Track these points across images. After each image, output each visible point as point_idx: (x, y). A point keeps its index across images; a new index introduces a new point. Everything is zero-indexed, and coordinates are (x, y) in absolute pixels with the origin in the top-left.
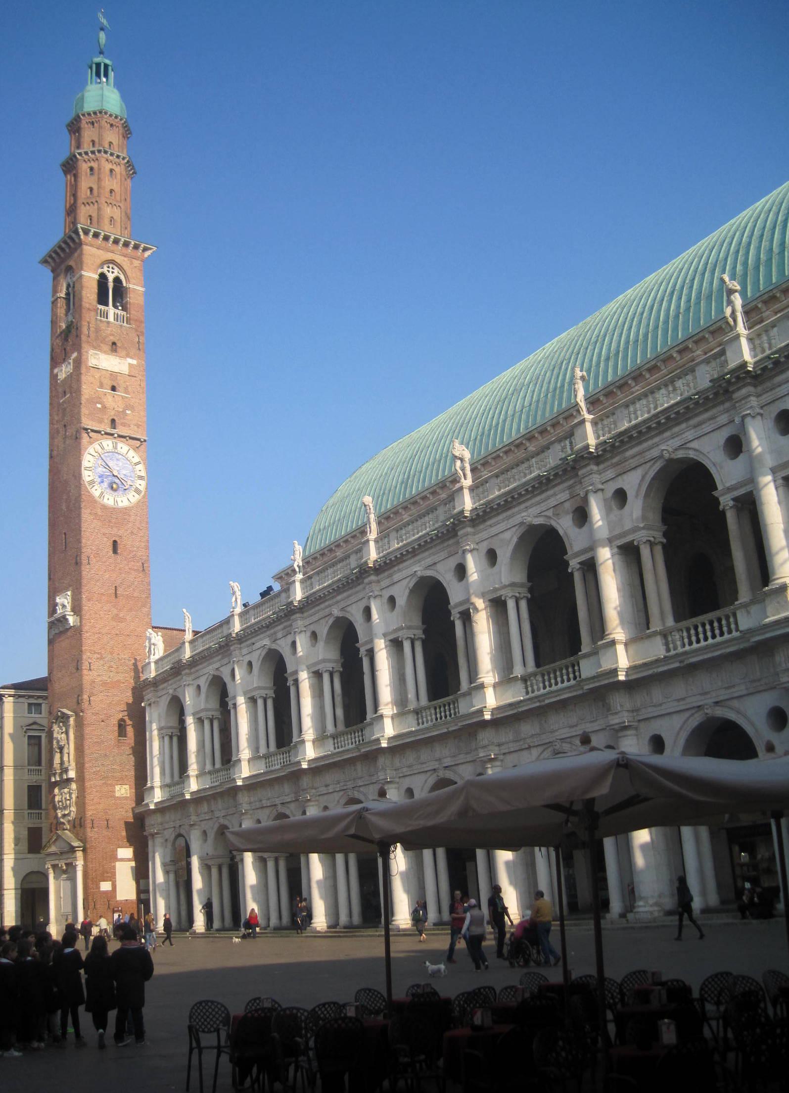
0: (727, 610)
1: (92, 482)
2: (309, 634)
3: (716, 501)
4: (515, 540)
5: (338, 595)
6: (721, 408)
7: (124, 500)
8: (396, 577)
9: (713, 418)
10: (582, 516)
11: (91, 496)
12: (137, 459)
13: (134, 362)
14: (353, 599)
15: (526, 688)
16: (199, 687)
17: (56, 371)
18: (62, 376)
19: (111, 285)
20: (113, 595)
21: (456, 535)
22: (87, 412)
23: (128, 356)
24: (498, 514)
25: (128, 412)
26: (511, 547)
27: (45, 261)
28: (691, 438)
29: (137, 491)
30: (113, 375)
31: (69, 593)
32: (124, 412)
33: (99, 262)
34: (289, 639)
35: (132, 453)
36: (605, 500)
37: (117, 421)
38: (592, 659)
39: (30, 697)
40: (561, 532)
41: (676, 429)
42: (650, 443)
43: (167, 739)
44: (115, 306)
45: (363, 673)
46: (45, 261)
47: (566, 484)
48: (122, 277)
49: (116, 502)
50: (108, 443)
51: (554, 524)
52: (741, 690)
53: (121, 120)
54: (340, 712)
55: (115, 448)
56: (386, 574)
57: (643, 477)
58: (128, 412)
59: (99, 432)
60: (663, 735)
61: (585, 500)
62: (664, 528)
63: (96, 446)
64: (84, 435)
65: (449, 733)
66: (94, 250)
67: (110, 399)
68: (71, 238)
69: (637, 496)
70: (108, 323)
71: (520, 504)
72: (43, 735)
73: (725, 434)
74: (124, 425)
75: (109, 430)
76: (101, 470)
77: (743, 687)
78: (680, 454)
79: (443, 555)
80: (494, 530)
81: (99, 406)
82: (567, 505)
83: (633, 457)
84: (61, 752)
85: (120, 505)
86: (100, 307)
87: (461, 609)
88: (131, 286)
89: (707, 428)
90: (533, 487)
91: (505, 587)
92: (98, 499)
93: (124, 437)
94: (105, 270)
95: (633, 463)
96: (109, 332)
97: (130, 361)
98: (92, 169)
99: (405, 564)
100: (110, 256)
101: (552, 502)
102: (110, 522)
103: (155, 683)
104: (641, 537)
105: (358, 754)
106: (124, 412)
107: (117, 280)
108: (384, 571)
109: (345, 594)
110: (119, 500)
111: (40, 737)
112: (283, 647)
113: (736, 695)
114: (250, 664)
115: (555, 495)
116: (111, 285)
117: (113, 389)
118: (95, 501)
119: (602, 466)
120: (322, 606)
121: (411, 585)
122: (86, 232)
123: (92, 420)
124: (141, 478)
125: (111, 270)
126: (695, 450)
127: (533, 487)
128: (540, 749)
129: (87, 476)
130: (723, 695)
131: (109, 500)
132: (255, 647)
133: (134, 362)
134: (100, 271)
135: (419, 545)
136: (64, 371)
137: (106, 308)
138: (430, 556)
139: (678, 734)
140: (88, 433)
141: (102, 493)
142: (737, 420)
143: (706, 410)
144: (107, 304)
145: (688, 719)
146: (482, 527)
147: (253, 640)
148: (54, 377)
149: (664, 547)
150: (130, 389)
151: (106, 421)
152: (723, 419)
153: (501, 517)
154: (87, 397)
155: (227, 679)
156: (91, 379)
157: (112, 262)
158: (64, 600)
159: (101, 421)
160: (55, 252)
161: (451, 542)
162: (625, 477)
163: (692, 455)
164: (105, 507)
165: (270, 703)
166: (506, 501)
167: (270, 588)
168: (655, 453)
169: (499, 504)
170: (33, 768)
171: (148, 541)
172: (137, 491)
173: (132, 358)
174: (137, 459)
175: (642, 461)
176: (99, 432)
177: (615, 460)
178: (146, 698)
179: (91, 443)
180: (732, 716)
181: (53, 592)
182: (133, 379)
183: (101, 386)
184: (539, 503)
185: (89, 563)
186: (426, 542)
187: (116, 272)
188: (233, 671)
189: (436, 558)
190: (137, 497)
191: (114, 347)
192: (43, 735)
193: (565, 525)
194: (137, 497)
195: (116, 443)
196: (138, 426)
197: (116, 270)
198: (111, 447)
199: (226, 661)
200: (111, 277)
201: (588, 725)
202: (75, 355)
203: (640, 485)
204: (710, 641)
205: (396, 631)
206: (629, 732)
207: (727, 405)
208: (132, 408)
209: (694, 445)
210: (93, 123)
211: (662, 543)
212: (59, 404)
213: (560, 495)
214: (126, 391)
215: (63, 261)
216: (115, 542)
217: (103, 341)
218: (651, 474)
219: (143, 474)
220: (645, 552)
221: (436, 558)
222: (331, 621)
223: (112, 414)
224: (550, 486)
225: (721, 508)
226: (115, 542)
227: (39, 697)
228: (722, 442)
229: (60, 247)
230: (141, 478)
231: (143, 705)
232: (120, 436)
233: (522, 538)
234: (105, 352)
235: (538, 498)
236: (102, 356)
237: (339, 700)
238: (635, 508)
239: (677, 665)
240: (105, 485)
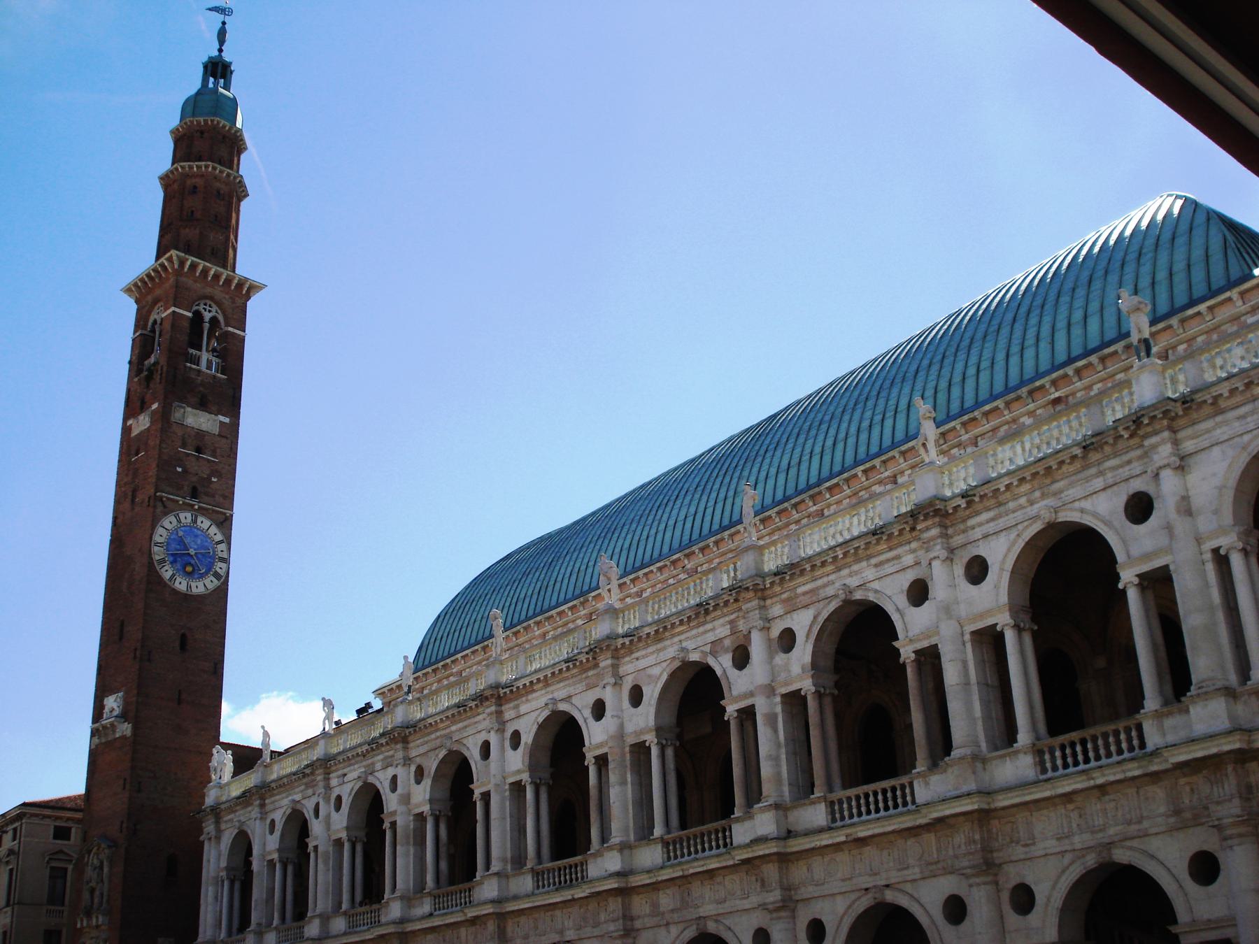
0: (904, 780)
1: (162, 561)
2: (413, 768)
3: (897, 653)
4: (665, 677)
5: (453, 723)
6: (907, 548)
7: (198, 587)
8: (524, 708)
9: (898, 557)
10: (742, 658)
12: (219, 537)
13: (227, 420)
14: (471, 731)
15: (668, 852)
16: (273, 821)
17: (129, 423)
18: (135, 433)
19: (206, 326)
21: (596, 666)
24: (648, 646)
26: (660, 685)
27: (128, 290)
28: (871, 577)
29: (217, 576)
30: (200, 434)
31: (120, 694)
34: (390, 772)
35: (214, 530)
36: (769, 640)
38: (747, 824)
39: (57, 818)
40: (719, 672)
41: (855, 567)
42: (825, 580)
43: (226, 883)
45: (476, 821)
46: (128, 290)
47: (727, 619)
48: (221, 318)
49: (189, 587)
50: (186, 517)
51: (711, 661)
52: (915, 872)
54: (444, 865)
55: (195, 522)
56: (512, 705)
57: (815, 617)
60: (824, 920)
61: (748, 637)
62: (836, 677)
64: (159, 504)
65: (573, 900)
68: (162, 265)
69: (808, 636)
70: (199, 371)
71: (673, 636)
72: (70, 867)
73: (910, 576)
74: (207, 494)
77: (917, 870)
78: (858, 596)
79: (580, 687)
80: (642, 663)
81: (179, 470)
82: (727, 642)
83: (805, 594)
84: (92, 891)
85: (195, 591)
86: (191, 351)
87: (599, 752)
88: (230, 329)
89: (889, 569)
90: (689, 617)
91: (651, 730)
93: (207, 509)
94: (201, 308)
95: (806, 599)
97: (222, 418)
98: (195, 187)
99: (534, 695)
100: (208, 290)
101: (710, 637)
103: (216, 811)
104: (806, 685)
105: (463, 919)
107: (214, 321)
108: (510, 700)
109: (460, 725)
110: (193, 585)
111: (66, 869)
112: (382, 780)
113: (910, 878)
114: (339, 799)
115: (713, 629)
116: (206, 326)
117: (199, 450)
119: (769, 602)
120: (433, 736)
121: (541, 720)
122: (182, 263)
126: (876, 591)
127: (689, 617)
128: (681, 927)
129: (158, 553)
130: (894, 877)
131: (181, 585)
132: (346, 779)
133: (227, 420)
134: (195, 308)
135: (553, 673)
136: (142, 423)
138: (564, 687)
139: (842, 918)
141: (173, 575)
142: (924, 563)
143: (891, 549)
144: (200, 350)
145: (854, 902)
146: (627, 659)
147: (345, 771)
148: (126, 430)
149: (835, 699)
152: (908, 560)
153: (650, 650)
155: (309, 814)
157: (212, 298)
158: (112, 703)
160: (142, 280)
161: (591, 673)
162: (795, 615)
163: (872, 597)
164: (176, 592)
165: (359, 848)
166: (657, 631)
167: (368, 705)
168: (830, 591)
169: (648, 634)
170: (53, 908)
172: (217, 576)
175: (814, 599)
177: (784, 596)
178: (205, 830)
179: (166, 514)
180: (904, 902)
181: (102, 692)
182: (224, 440)
184: (695, 637)
185: (149, 660)
186: (561, 670)
188: (318, 804)
189: (571, 690)
192: (70, 867)
193: (722, 664)
196: (225, 497)
197: (215, 308)
198: (189, 520)
199: (310, 792)
200: (207, 316)
201: (738, 902)
202: (155, 406)
203: (811, 627)
204: (882, 813)
205: (519, 772)
206: (783, 914)
207: (914, 545)
209: (876, 585)
210: (202, 133)
211: (833, 695)
212: (130, 462)
213: (719, 629)
215: (150, 291)
216: (183, 639)
218: (825, 614)
220: (812, 704)
221: (571, 690)
222: (442, 753)
224: (708, 618)
225: (902, 660)
226: (183, 639)
227: (68, 819)
228: (906, 585)
229: (148, 275)
231: (201, 838)
233: (673, 675)
235: (694, 632)
237: (443, 850)
238: (803, 652)
239: (843, 839)
240: (178, 566)
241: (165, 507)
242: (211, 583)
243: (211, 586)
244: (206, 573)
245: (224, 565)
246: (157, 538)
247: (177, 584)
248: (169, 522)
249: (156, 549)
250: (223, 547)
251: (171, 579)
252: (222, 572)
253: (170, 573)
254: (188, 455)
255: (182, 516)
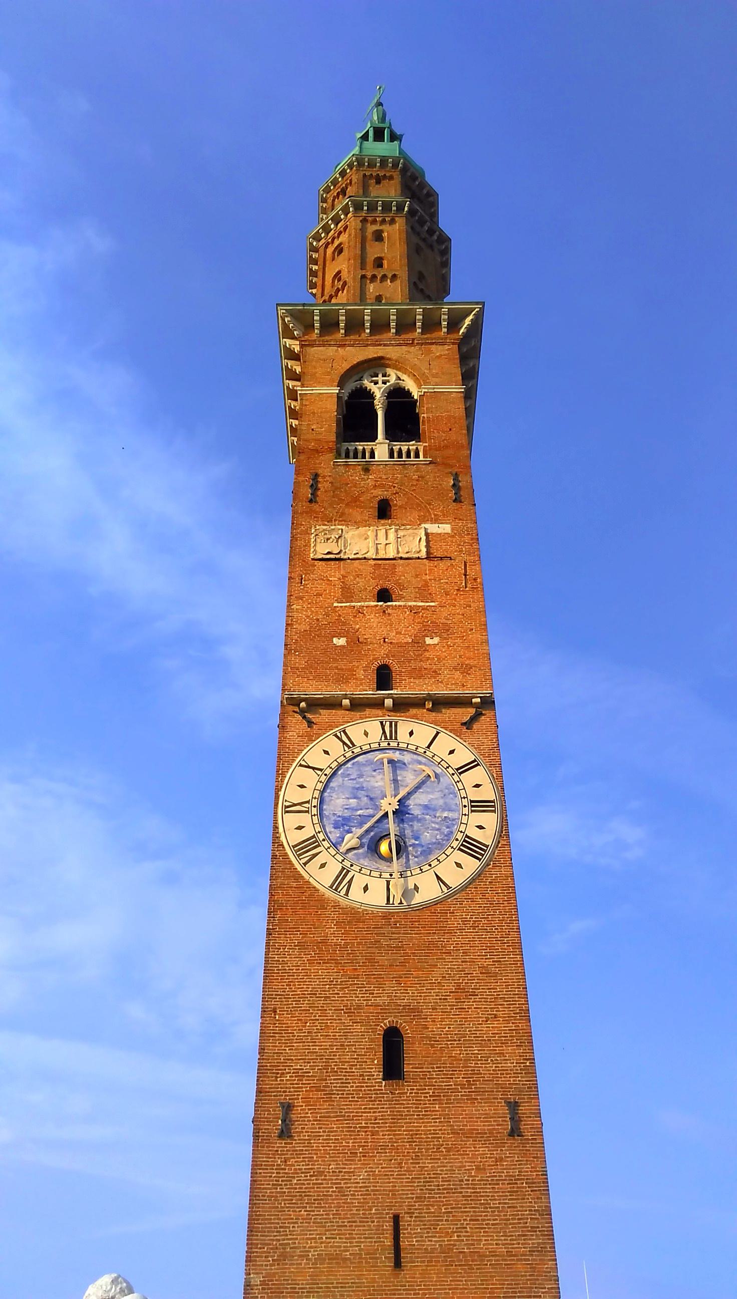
1: (308, 847)
11: (306, 888)
13: (446, 528)
20: (386, 1259)
22: (303, 663)
23: (423, 520)
25: (428, 641)
29: (470, 846)
30: (384, 564)
32: (418, 642)
33: (346, 366)
35: (446, 741)
37: (395, 667)
44: (391, 435)
48: (410, 385)
50: (366, 731)
53: (395, 165)
55: (394, 736)
58: (428, 641)
59: (332, 704)
63: (330, 742)
66: (331, 351)
67: (374, 619)
74: (418, 674)
75: (369, 692)
76: (338, 803)
81: (341, 642)
92: (330, 894)
96: (371, 483)
100: (371, 352)
102: (371, 961)
106: (418, 642)
117: (384, 595)
118: (322, 902)
123: (318, 678)
124: (479, 806)
125: (380, 378)
131: (370, 891)
133: (446, 528)
137: (368, 446)
140: (302, 712)
144: (374, 438)
150: (434, 587)
151: (361, 674)
154: (304, 627)
156: (321, 586)
159: (343, 678)
164: (355, 917)
171: (525, 1015)
172: (470, 846)
173: (436, 520)
174: (464, 756)
176: (332, 704)
182: (442, 565)
183: (347, 594)
187: (393, 380)
190: (471, 865)
191: (384, 511)
194: (471, 865)
195: (394, 726)
196: (466, 669)
208: (444, 631)
214: (424, 592)
217: (355, 501)
219: (488, 793)
223: (381, 654)
230: (479, 806)
232: (402, 706)
234: (358, 524)
236: (351, 534)
241: (310, 723)
242: (457, 868)
243: (455, 879)
244: (439, 845)
245: (490, 820)
246: (291, 794)
247: (356, 894)
248: (323, 752)
249: (291, 820)
250: (479, 774)
251: (335, 886)
252: (487, 837)
253: (334, 868)
254: (360, 611)
255: (355, 732)
